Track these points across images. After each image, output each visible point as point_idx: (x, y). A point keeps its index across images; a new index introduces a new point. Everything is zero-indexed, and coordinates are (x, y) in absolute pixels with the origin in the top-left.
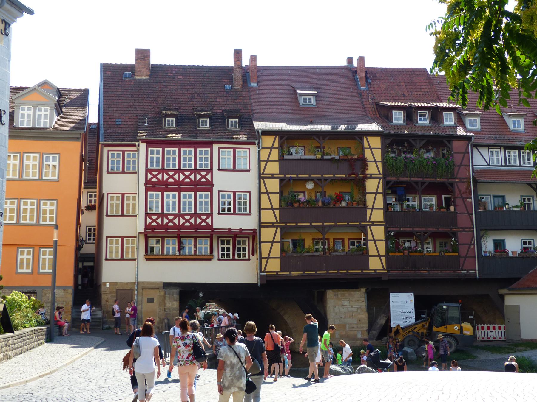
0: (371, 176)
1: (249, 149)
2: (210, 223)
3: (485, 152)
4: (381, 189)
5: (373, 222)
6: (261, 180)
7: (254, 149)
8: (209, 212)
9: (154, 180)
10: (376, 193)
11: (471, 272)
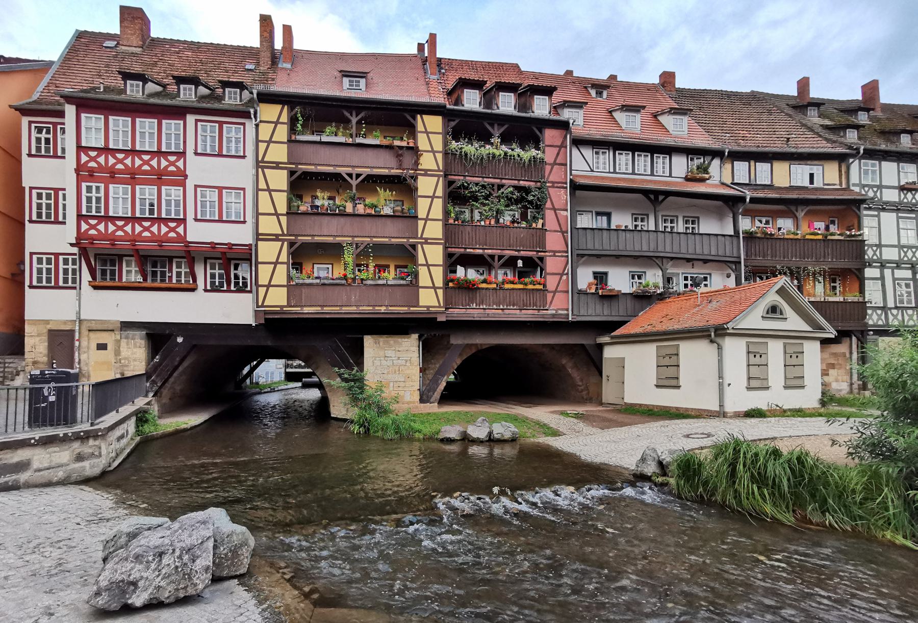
0: (426, 173)
1: (244, 124)
2: (183, 234)
3: (588, 152)
4: (440, 192)
5: (426, 239)
6: (260, 170)
7: (250, 125)
8: (182, 217)
9: (93, 164)
10: (433, 197)
11: (560, 312)
